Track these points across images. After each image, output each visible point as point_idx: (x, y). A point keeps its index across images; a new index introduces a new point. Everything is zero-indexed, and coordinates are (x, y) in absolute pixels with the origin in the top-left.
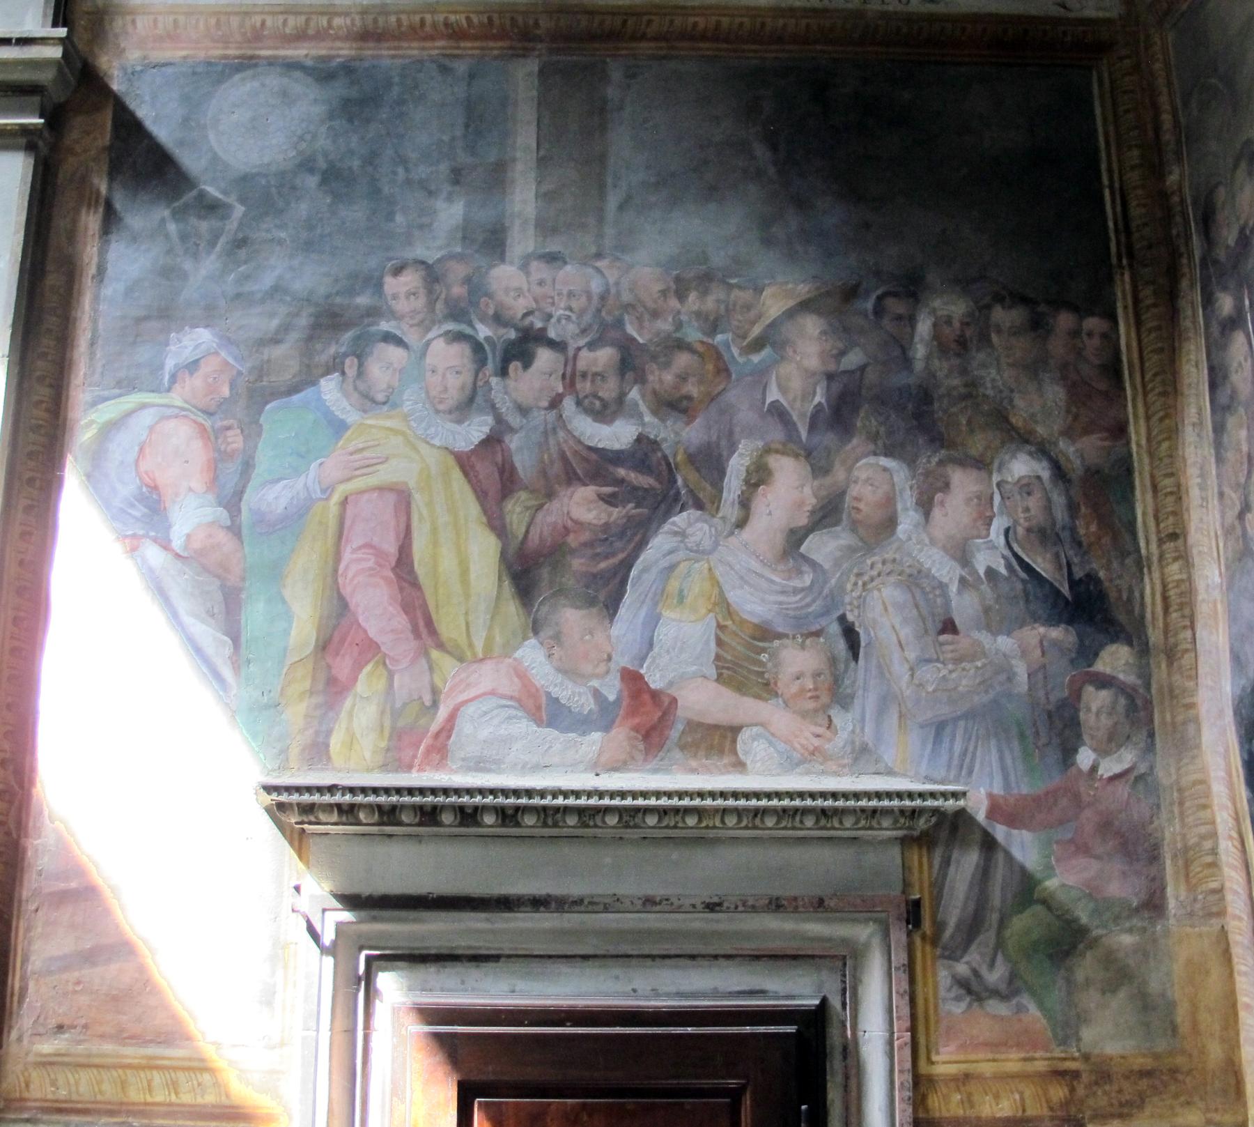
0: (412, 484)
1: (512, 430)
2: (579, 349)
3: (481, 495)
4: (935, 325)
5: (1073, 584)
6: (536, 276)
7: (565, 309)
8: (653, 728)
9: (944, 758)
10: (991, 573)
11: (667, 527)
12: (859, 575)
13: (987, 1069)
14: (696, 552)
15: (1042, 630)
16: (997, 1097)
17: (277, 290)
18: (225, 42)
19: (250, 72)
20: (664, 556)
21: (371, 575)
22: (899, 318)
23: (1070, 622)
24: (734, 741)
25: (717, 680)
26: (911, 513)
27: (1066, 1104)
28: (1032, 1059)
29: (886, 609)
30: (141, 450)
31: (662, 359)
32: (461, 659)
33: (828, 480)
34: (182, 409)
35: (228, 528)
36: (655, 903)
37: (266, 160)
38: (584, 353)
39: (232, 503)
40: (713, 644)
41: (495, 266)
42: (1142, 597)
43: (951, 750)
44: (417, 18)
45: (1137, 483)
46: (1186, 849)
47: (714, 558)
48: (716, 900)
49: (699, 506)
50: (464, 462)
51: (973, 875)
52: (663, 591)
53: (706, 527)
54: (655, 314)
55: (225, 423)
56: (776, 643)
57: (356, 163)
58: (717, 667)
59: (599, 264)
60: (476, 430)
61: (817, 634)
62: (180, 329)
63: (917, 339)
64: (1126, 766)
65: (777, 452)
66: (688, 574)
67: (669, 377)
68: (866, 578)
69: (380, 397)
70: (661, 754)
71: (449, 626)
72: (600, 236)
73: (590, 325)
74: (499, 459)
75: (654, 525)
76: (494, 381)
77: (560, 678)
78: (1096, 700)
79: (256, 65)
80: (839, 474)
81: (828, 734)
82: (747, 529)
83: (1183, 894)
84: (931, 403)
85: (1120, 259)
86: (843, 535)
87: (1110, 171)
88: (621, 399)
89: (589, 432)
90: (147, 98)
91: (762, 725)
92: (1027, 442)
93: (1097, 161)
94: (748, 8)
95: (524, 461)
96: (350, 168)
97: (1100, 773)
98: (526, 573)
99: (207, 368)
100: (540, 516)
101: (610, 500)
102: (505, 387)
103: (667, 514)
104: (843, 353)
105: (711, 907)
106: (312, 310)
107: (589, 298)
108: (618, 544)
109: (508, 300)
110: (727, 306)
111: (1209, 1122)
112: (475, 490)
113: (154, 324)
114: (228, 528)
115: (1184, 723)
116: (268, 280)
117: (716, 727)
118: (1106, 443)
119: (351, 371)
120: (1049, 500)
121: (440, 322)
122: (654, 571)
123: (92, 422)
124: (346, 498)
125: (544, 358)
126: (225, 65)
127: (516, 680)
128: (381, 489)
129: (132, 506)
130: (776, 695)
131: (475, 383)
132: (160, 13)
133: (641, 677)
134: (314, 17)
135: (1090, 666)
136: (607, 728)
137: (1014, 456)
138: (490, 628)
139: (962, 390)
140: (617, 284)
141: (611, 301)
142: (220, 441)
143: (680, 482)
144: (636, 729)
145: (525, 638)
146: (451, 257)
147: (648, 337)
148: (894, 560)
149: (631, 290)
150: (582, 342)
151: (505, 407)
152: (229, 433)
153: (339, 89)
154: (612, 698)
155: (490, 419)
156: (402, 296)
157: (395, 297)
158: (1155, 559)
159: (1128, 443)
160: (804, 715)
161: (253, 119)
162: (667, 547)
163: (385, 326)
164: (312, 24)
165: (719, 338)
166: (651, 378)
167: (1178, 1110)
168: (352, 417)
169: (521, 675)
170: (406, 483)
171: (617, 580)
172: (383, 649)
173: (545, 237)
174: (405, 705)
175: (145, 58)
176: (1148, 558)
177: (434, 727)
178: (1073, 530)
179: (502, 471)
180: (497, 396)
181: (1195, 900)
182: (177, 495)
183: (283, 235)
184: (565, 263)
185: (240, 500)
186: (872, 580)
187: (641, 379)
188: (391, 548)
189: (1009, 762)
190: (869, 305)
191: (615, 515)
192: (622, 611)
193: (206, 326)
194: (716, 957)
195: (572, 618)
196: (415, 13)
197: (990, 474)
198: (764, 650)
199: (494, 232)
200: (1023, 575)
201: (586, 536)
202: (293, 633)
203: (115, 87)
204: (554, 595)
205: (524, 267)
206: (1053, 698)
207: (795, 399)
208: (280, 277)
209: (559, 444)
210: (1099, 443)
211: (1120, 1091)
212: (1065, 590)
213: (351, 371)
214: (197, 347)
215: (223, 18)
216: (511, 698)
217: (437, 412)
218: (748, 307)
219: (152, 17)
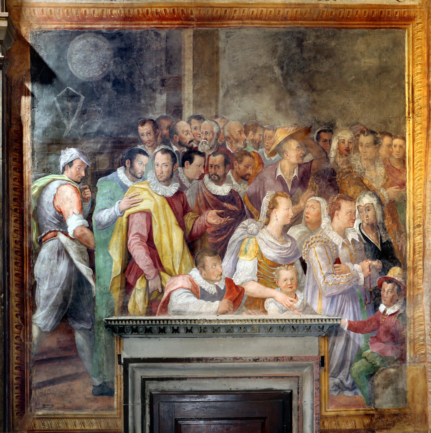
0: (152, 210)
1: (186, 188)
2: (210, 155)
3: (176, 214)
4: (338, 143)
5: (382, 244)
6: (193, 126)
7: (204, 139)
8: (236, 299)
10: (353, 240)
11: (241, 225)
12: (308, 242)
13: (344, 413)
14: (251, 234)
15: (370, 262)
16: (347, 422)
17: (99, 132)
18: (71, 20)
19: (82, 36)
20: (240, 236)
21: (139, 245)
22: (325, 141)
23: (380, 259)
24: (263, 303)
25: (258, 282)
26: (327, 219)
27: (369, 425)
28: (359, 410)
29: (316, 255)
30: (55, 198)
31: (239, 159)
32: (171, 275)
33: (297, 206)
34: (68, 181)
35: (88, 228)
36: (237, 359)
37: (91, 75)
38: (211, 157)
39: (89, 218)
40: (256, 269)
41: (179, 121)
42: (406, 248)
43: (337, 305)
44: (146, 9)
45: (408, 205)
46: (414, 339)
47: (258, 236)
48: (257, 358)
49: (252, 217)
50: (170, 200)
52: (240, 249)
53: (255, 225)
54: (237, 141)
55: (84, 186)
56: (278, 268)
57: (125, 77)
58: (258, 277)
59: (216, 120)
60: (172, 189)
61: (292, 264)
62: (64, 149)
63: (331, 149)
64: (396, 311)
65: (280, 195)
66: (248, 243)
67: (242, 167)
68: (310, 243)
69: (139, 176)
70: (239, 308)
71: (167, 263)
72: (217, 108)
73: (214, 146)
74: (182, 200)
75: (237, 225)
76: (179, 169)
77: (205, 282)
78: (387, 287)
79: (84, 32)
80: (302, 204)
81: (295, 300)
82: (269, 225)
84: (336, 175)
85: (409, 114)
86: (302, 227)
87: (409, 75)
88: (225, 175)
89: (213, 188)
90: (43, 47)
91: (273, 297)
92: (369, 190)
93: (404, 71)
94: (274, 4)
95: (191, 202)
96: (123, 79)
98: (192, 243)
99: (76, 164)
100: (197, 221)
101: (221, 215)
102: (184, 171)
103: (241, 220)
104: (304, 156)
105: (255, 360)
106: (112, 140)
107: (213, 134)
108: (224, 232)
109: (183, 136)
110: (263, 137)
111: (415, 431)
112: (173, 211)
113: (55, 146)
114: (88, 228)
115: (417, 295)
116: (95, 128)
117: (257, 298)
118: (398, 190)
119: (128, 166)
120: (376, 213)
121: (159, 145)
122: (237, 242)
123: (36, 186)
124: (129, 216)
125: (197, 159)
126: (72, 32)
127: (190, 282)
128: (141, 212)
129: (54, 219)
130: (278, 287)
131: (173, 170)
132: (44, 7)
133: (232, 281)
134: (105, 9)
136: (221, 300)
137: (364, 196)
138: (181, 264)
139: (347, 170)
140: (223, 128)
141: (221, 136)
143: (245, 208)
144: (230, 299)
145: (193, 267)
146: (162, 117)
147: (234, 150)
148: (320, 237)
149: (229, 131)
150: (210, 153)
151: (184, 179)
152: (86, 191)
153: (117, 43)
154: (222, 288)
155: (178, 184)
156: (145, 134)
157: (143, 135)
158: (412, 234)
159: (406, 190)
160: (287, 294)
161: (85, 57)
162: (241, 233)
163: (139, 147)
164: (105, 12)
165: (260, 150)
166: (235, 167)
167: (406, 427)
168: (129, 184)
169: (192, 281)
170: (149, 210)
171: (224, 246)
172: (144, 272)
173: (197, 109)
174: (153, 292)
175: (40, 28)
176: (409, 234)
177: (163, 300)
178: (383, 224)
179: (183, 205)
180: (181, 175)
182: (69, 215)
183: (100, 109)
184: (204, 120)
186: (312, 244)
187: (232, 168)
188: (145, 233)
189: (356, 310)
190: (315, 136)
191: (223, 221)
192: (226, 257)
193: (74, 147)
194: (257, 377)
195: (209, 260)
196: (144, 7)
197: (355, 202)
198: (274, 270)
199: (177, 107)
200: (365, 241)
201: (213, 229)
202: (113, 266)
203: (30, 42)
204: (202, 251)
205: (189, 122)
206: (372, 286)
207: (287, 175)
208: (100, 127)
209: (203, 194)
210: (395, 190)
211: (387, 421)
212: (379, 247)
213: (128, 166)
214: (72, 155)
215: (70, 10)
216: (188, 289)
217: (160, 181)
218: (271, 137)
219: (41, 9)
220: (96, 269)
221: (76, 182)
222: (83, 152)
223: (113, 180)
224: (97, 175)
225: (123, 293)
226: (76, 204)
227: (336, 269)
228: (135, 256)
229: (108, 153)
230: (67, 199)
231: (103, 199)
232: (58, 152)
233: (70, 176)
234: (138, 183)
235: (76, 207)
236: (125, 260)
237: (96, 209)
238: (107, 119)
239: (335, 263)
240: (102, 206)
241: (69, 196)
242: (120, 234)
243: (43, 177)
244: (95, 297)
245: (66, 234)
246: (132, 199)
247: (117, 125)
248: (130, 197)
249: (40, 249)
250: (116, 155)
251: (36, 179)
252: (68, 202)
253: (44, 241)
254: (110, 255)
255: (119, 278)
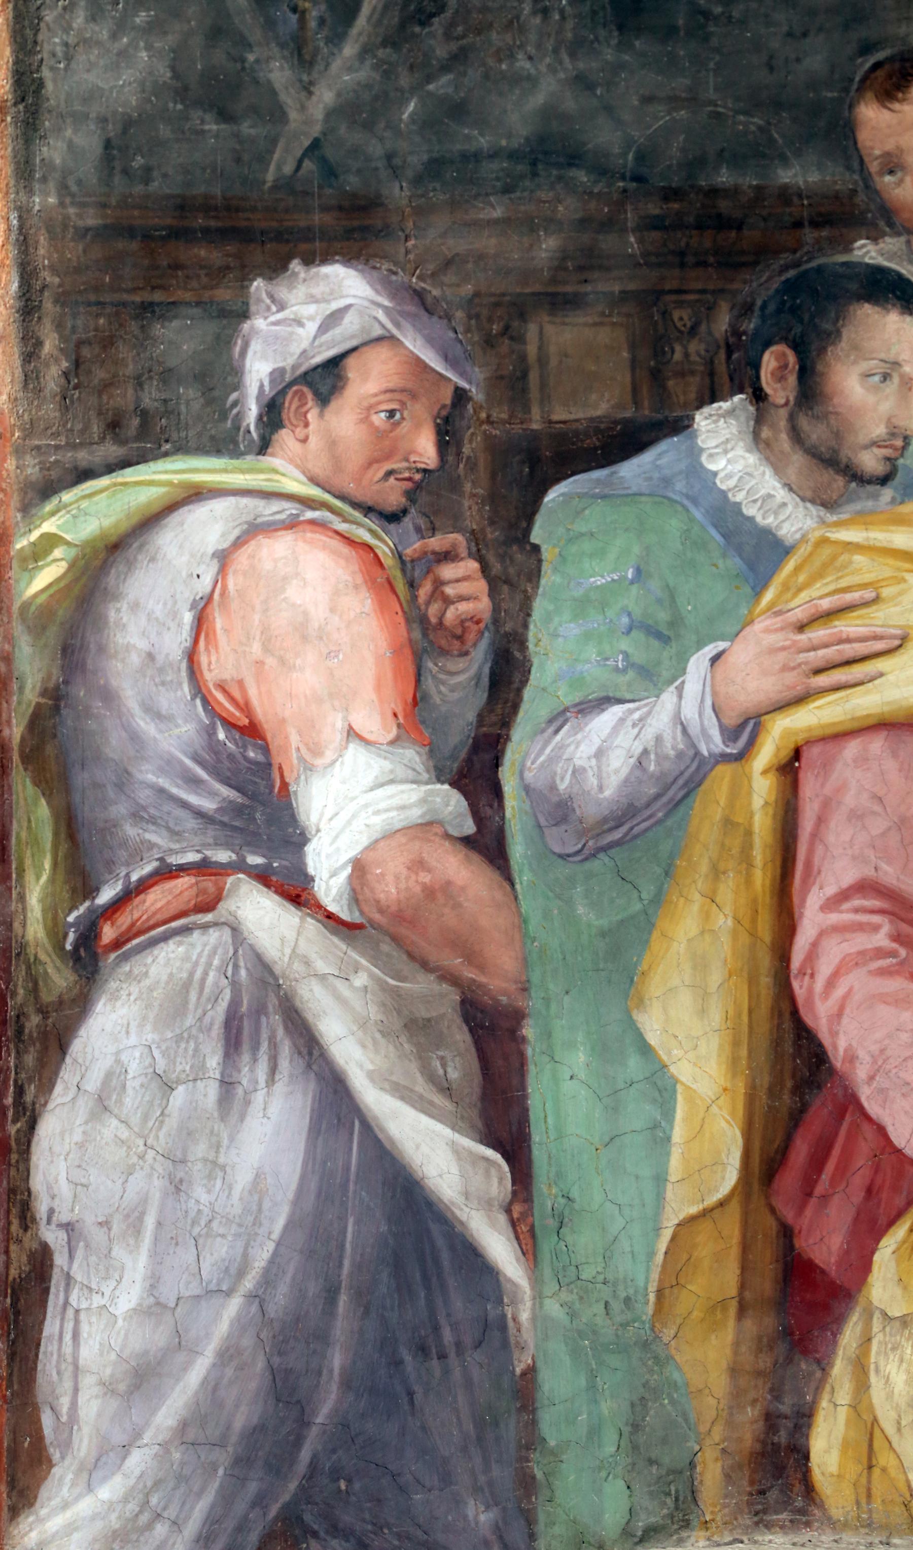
17: (550, 152)
21: (883, 972)
30: (201, 623)
35: (467, 841)
39: (476, 769)
55: (436, 543)
69: (870, 462)
99: (369, 380)
114: (467, 841)
116: (516, 118)
124: (797, 754)
129: (193, 782)
142: (424, 592)
152: (448, 571)
163: (868, 252)
168: (793, 520)
182: (317, 751)
185: (497, 763)
202: (678, 1134)
208: (548, 113)
213: (781, 393)
214: (333, 319)
220: (539, 1154)
221: (368, 510)
222: (420, 296)
223: (659, 491)
224: (533, 459)
225: (762, 1345)
226: (369, 672)
228: (851, 1058)
229: (625, 296)
230: (302, 631)
231: (587, 636)
232: (223, 294)
233: (320, 467)
234: (862, 519)
235: (368, 692)
236: (773, 1092)
237: (534, 706)
238: (609, 54)
240: (577, 681)
241: (319, 613)
242: (727, 891)
243: (110, 469)
244: (531, 1372)
245: (297, 893)
246: (818, 634)
247: (692, 100)
248: (799, 614)
249: (80, 1004)
250: (682, 316)
251: (47, 489)
252: (310, 656)
253: (117, 944)
254: (645, 1049)
255: (731, 1225)
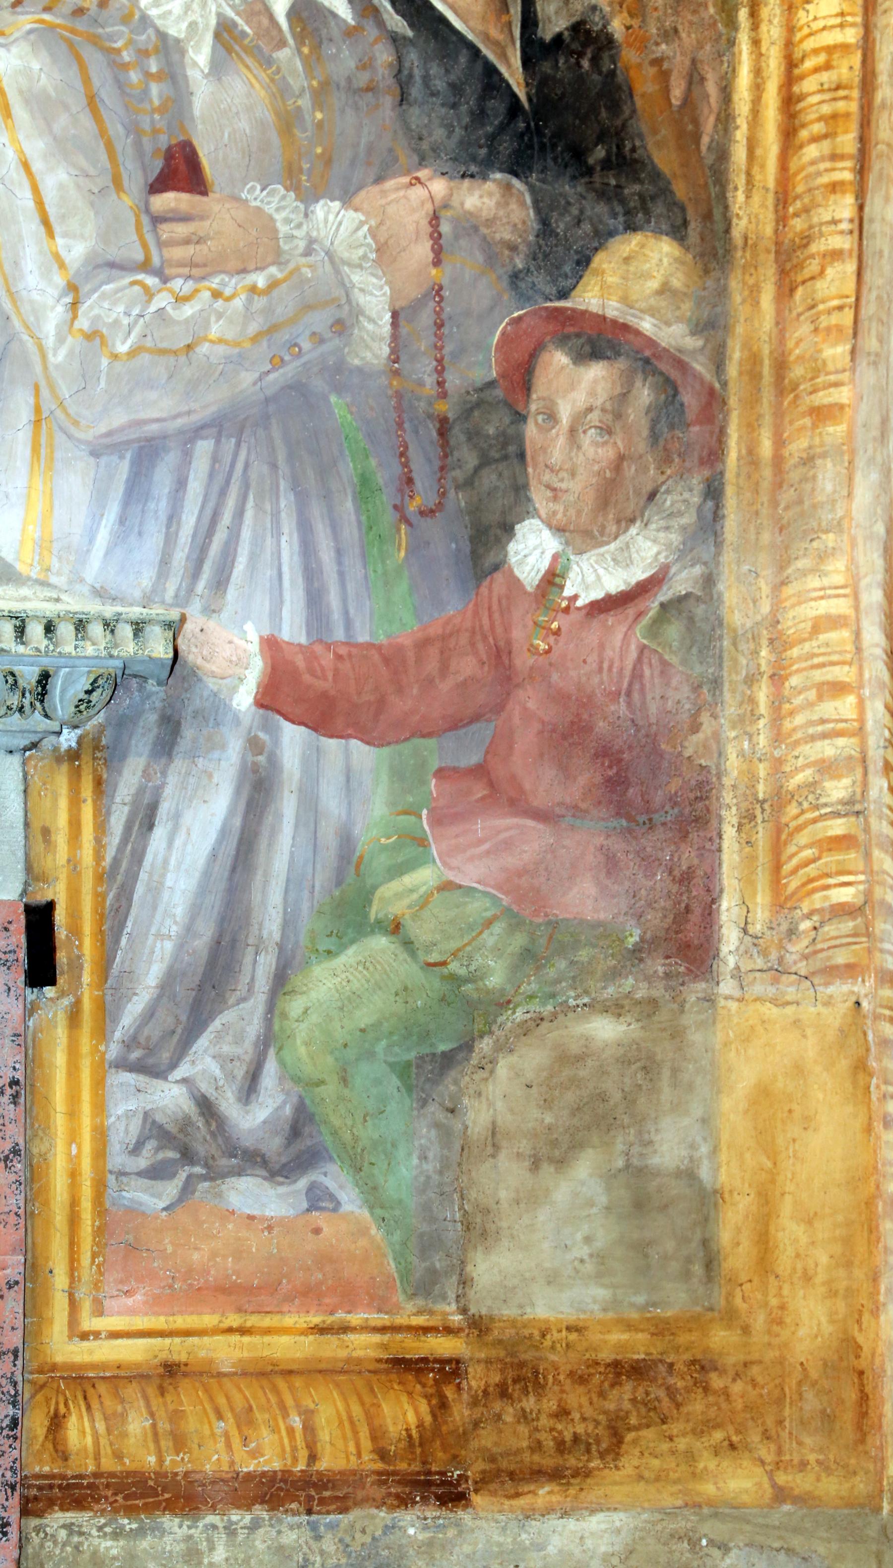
9: (154, 539)
15: (439, 187)
23: (517, 167)
51: (213, 856)
64: (639, 574)
78: (574, 387)
83: (761, 916)
97: (568, 592)
111: (781, 1495)
135: (564, 294)
167: (707, 1462)
181: (792, 932)
212: (513, 72)
227: (167, 231)
239: (158, 186)
